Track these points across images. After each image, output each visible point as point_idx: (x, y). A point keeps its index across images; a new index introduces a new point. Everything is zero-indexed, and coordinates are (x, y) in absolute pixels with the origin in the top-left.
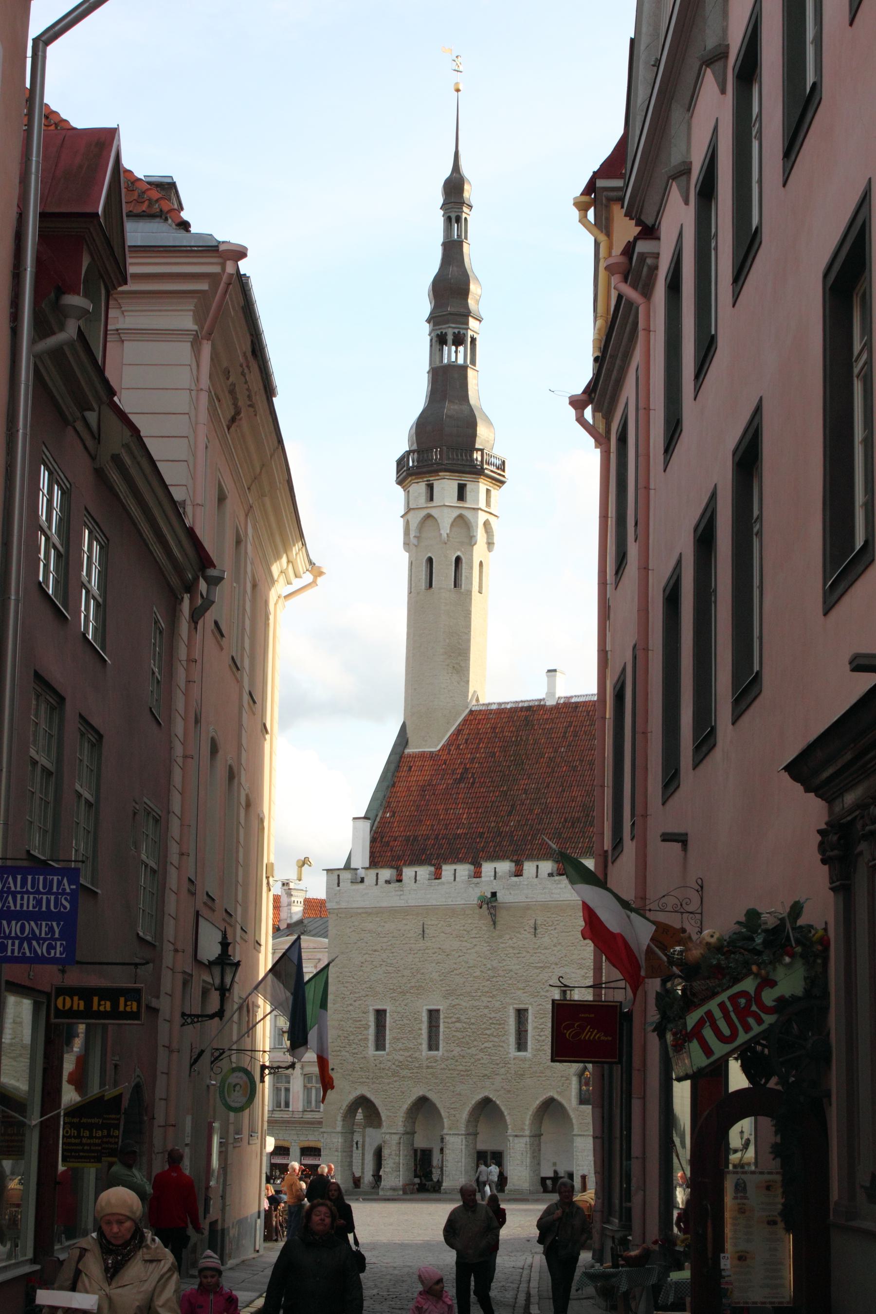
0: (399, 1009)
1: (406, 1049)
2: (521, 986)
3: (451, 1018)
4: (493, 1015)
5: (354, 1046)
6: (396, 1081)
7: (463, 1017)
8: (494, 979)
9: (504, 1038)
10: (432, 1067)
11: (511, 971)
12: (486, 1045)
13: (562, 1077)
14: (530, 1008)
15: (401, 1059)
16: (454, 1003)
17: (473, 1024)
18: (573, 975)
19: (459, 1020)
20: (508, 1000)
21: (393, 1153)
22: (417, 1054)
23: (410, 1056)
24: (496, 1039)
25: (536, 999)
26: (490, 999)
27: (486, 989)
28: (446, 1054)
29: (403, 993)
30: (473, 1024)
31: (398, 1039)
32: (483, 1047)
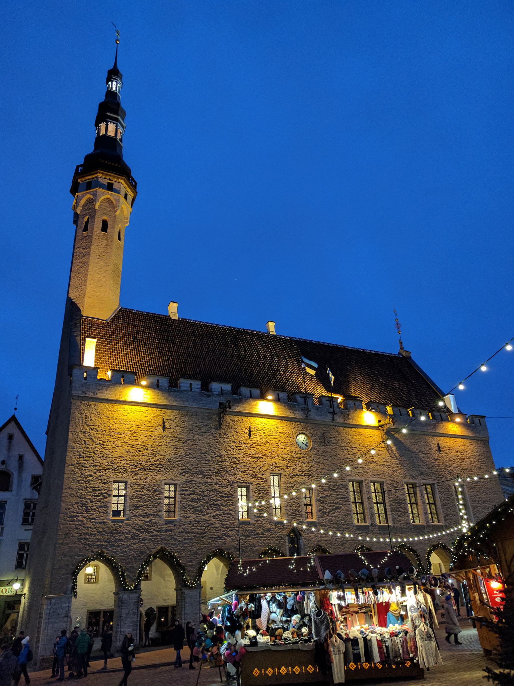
0: (140, 482)
1: (147, 515)
2: (242, 470)
3: (187, 490)
4: (222, 489)
5: (92, 512)
6: (135, 544)
7: (197, 491)
8: (222, 464)
9: (231, 508)
10: (171, 530)
11: (235, 458)
12: (217, 512)
13: (278, 537)
14: (251, 486)
15: (141, 523)
16: (189, 479)
17: (206, 496)
18: (280, 465)
19: (193, 492)
20: (233, 479)
21: (131, 612)
22: (156, 520)
23: (150, 521)
24: (225, 508)
25: (254, 480)
26: (219, 478)
27: (217, 470)
28: (183, 520)
29: (144, 469)
30: (206, 496)
31: (138, 507)
32: (214, 514)
